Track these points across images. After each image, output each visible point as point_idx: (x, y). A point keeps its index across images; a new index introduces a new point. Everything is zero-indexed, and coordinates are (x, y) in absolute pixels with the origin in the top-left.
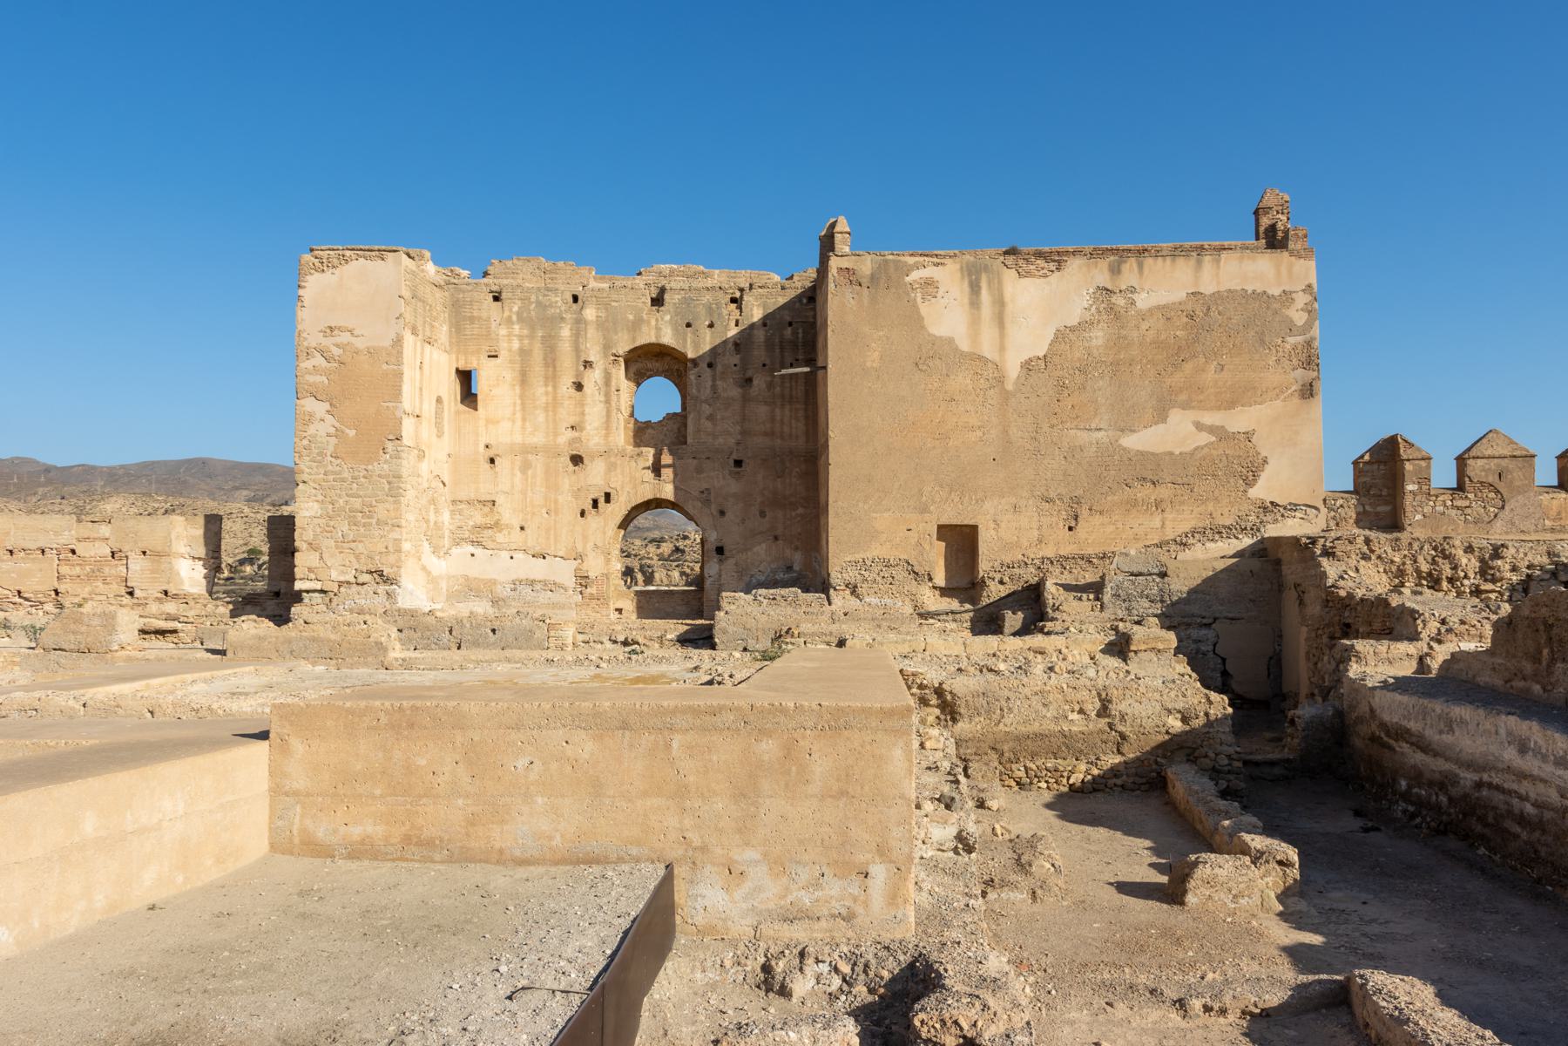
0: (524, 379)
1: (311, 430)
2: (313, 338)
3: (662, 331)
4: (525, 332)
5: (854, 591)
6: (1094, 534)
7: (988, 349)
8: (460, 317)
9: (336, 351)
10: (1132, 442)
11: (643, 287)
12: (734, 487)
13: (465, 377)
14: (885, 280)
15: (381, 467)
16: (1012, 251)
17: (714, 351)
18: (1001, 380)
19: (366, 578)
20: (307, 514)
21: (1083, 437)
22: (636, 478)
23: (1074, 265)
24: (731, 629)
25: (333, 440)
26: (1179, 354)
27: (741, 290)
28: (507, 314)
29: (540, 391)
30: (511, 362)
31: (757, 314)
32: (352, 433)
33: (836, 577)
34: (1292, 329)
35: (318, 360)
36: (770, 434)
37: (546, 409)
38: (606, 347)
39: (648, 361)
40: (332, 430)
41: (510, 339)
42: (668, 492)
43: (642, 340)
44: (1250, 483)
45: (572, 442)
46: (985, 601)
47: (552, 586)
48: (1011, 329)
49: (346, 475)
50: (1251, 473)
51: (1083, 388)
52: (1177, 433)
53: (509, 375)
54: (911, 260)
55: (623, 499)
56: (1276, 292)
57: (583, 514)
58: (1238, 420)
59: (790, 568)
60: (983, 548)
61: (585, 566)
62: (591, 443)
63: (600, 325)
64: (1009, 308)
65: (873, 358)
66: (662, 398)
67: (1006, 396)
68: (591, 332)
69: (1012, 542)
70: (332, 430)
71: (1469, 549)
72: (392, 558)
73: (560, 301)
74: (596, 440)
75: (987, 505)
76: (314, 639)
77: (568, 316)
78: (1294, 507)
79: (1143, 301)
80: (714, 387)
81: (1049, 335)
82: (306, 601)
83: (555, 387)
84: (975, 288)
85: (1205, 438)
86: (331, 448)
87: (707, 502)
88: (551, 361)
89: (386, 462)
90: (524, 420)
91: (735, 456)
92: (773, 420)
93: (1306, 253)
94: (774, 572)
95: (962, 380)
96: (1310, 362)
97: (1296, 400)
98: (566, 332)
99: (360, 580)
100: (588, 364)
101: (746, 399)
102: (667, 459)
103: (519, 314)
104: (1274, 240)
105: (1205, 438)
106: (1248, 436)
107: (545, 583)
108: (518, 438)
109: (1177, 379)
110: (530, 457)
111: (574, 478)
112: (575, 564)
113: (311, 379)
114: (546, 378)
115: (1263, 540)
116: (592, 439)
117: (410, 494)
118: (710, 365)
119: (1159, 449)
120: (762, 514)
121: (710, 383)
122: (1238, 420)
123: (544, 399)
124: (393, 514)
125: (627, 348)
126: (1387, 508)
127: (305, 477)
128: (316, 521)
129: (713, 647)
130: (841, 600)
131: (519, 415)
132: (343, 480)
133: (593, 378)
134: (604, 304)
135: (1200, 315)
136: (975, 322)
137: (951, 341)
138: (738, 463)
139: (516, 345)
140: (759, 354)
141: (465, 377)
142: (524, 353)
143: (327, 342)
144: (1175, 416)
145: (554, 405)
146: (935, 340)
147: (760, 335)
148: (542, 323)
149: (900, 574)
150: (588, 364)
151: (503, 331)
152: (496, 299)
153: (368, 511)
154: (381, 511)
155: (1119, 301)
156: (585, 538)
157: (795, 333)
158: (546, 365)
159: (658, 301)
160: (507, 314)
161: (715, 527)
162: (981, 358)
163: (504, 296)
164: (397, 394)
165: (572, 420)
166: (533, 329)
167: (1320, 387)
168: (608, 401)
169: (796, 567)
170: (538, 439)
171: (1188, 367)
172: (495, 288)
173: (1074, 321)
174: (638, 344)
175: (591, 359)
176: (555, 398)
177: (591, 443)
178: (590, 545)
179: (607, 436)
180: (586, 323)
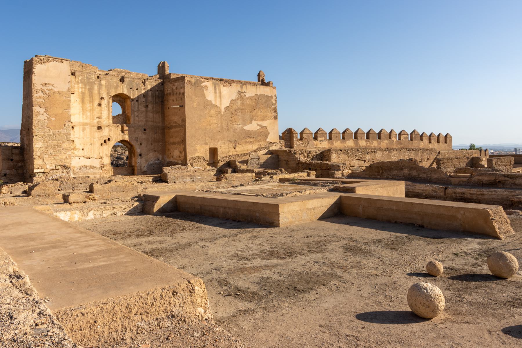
0: (83, 101)
1: (39, 118)
3: (124, 89)
4: (83, 86)
5: (192, 165)
6: (241, 149)
9: (47, 92)
10: (246, 128)
12: (144, 136)
14: (197, 84)
17: (138, 97)
18: (220, 112)
19: (59, 167)
20: (38, 146)
21: (236, 126)
22: (117, 134)
23: (234, 85)
24: (172, 177)
25: (47, 121)
26: (254, 108)
27: (145, 80)
28: (77, 80)
29: (88, 106)
30: (79, 96)
31: (149, 87)
32: (53, 119)
33: (189, 162)
35: (41, 94)
36: (153, 121)
37: (90, 112)
38: (108, 93)
40: (46, 118)
42: (127, 138)
43: (118, 92)
45: (98, 122)
46: (219, 167)
47: (93, 167)
49: (51, 133)
50: (267, 135)
51: (236, 115)
52: (253, 126)
53: (78, 100)
54: (203, 80)
55: (114, 140)
56: (270, 95)
57: (101, 144)
58: (265, 124)
59: (159, 159)
60: (218, 154)
61: (103, 161)
62: (104, 123)
64: (222, 94)
66: (118, 110)
67: (222, 116)
68: (104, 88)
69: (225, 152)
70: (46, 118)
71: (306, 152)
72: (68, 161)
73: (94, 77)
74: (106, 122)
75: (219, 143)
76: (119, 186)
77: (96, 83)
78: (274, 143)
79: (247, 95)
80: (138, 107)
81: (230, 102)
82: (37, 176)
83: (93, 105)
85: (259, 127)
86: (46, 124)
87: (137, 141)
88: (91, 96)
89: (65, 129)
90: (83, 114)
91: (144, 128)
92: (154, 118)
93: (275, 88)
94: (155, 161)
95: (213, 112)
96: (276, 112)
97: (274, 120)
98: (96, 87)
99: (57, 168)
100: (102, 98)
101: (147, 111)
102: (126, 128)
103: (81, 80)
104: (264, 83)
105: (259, 127)
106: (266, 127)
107: (90, 166)
108: (81, 120)
109: (254, 114)
110: (85, 127)
111: (99, 133)
112: (100, 160)
113: (38, 100)
114: (90, 102)
115: (270, 150)
118: (137, 101)
119: (251, 130)
120: (152, 144)
121: (137, 106)
122: (265, 124)
123: (89, 108)
124: (68, 146)
125: (114, 94)
126: (289, 143)
127: (37, 134)
128: (41, 149)
129: (167, 182)
130: (190, 168)
131: (81, 113)
132: (51, 135)
133: (104, 103)
134: (107, 80)
135: (257, 98)
136: (216, 97)
137: (211, 101)
138: (145, 130)
139: (80, 90)
140: (150, 99)
142: (83, 93)
143: (44, 88)
144: (253, 122)
145: (92, 110)
146: (208, 101)
147: (150, 93)
148: (88, 84)
149: (202, 161)
150: (102, 98)
151: (76, 86)
152: (72, 74)
153: (59, 145)
154: (65, 145)
155: (243, 95)
156: (103, 152)
157: (159, 93)
158: (90, 97)
159: (122, 80)
160: (77, 80)
161: (139, 148)
162: (217, 106)
163: (76, 74)
164: (69, 107)
165: (98, 115)
166: (85, 85)
167: (278, 117)
168: (109, 110)
169: (160, 159)
170: (88, 121)
171: (255, 111)
172: (73, 71)
173: (234, 99)
174: (117, 93)
175: (104, 96)
176: (93, 108)
177: (104, 123)
178: (104, 154)
179: (109, 120)
180: (102, 85)
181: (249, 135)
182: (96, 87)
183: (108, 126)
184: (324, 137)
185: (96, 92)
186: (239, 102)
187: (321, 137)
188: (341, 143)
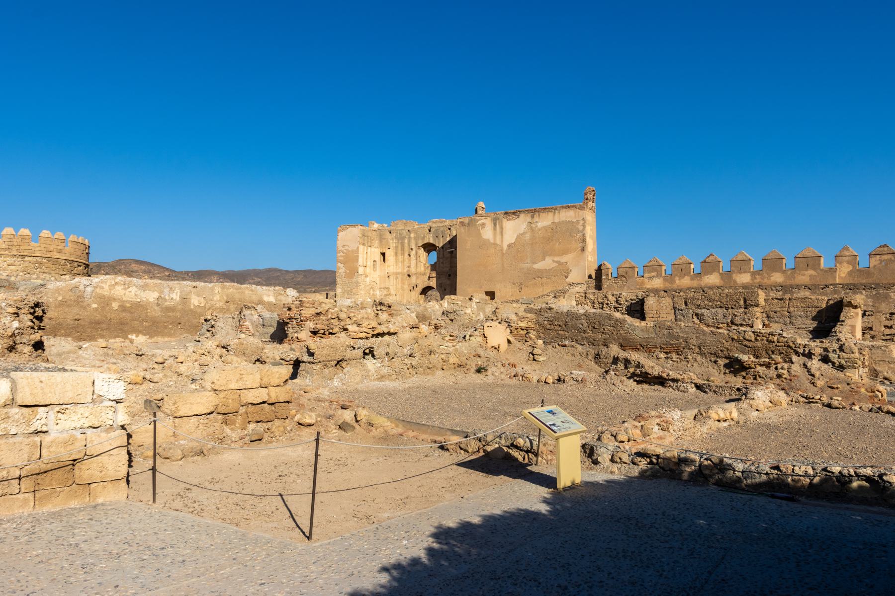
0: (396, 254)
2: (340, 248)
7: (498, 242)
8: (381, 239)
10: (536, 266)
11: (426, 226)
13: (383, 254)
15: (354, 280)
16: (506, 213)
18: (502, 250)
23: (522, 216)
29: (400, 257)
34: (579, 232)
39: (429, 248)
41: (393, 243)
44: (566, 277)
48: (505, 236)
52: (547, 263)
58: (563, 259)
63: (415, 238)
65: (468, 246)
67: (503, 254)
68: (413, 241)
73: (405, 233)
79: (540, 225)
81: (515, 236)
84: (495, 225)
85: (555, 265)
88: (403, 249)
95: (492, 251)
98: (406, 241)
105: (555, 265)
106: (566, 263)
116: (413, 270)
117: (362, 286)
122: (563, 259)
134: (416, 232)
135: (554, 229)
136: (495, 235)
141: (383, 254)
142: (396, 247)
145: (403, 261)
146: (484, 240)
148: (400, 239)
153: (351, 291)
154: (354, 291)
155: (533, 226)
170: (400, 270)
181: (540, 274)
182: (406, 241)
183: (416, 274)
184: (656, 271)
185: (406, 245)
186: (528, 236)
187: (650, 272)
188: (692, 279)
